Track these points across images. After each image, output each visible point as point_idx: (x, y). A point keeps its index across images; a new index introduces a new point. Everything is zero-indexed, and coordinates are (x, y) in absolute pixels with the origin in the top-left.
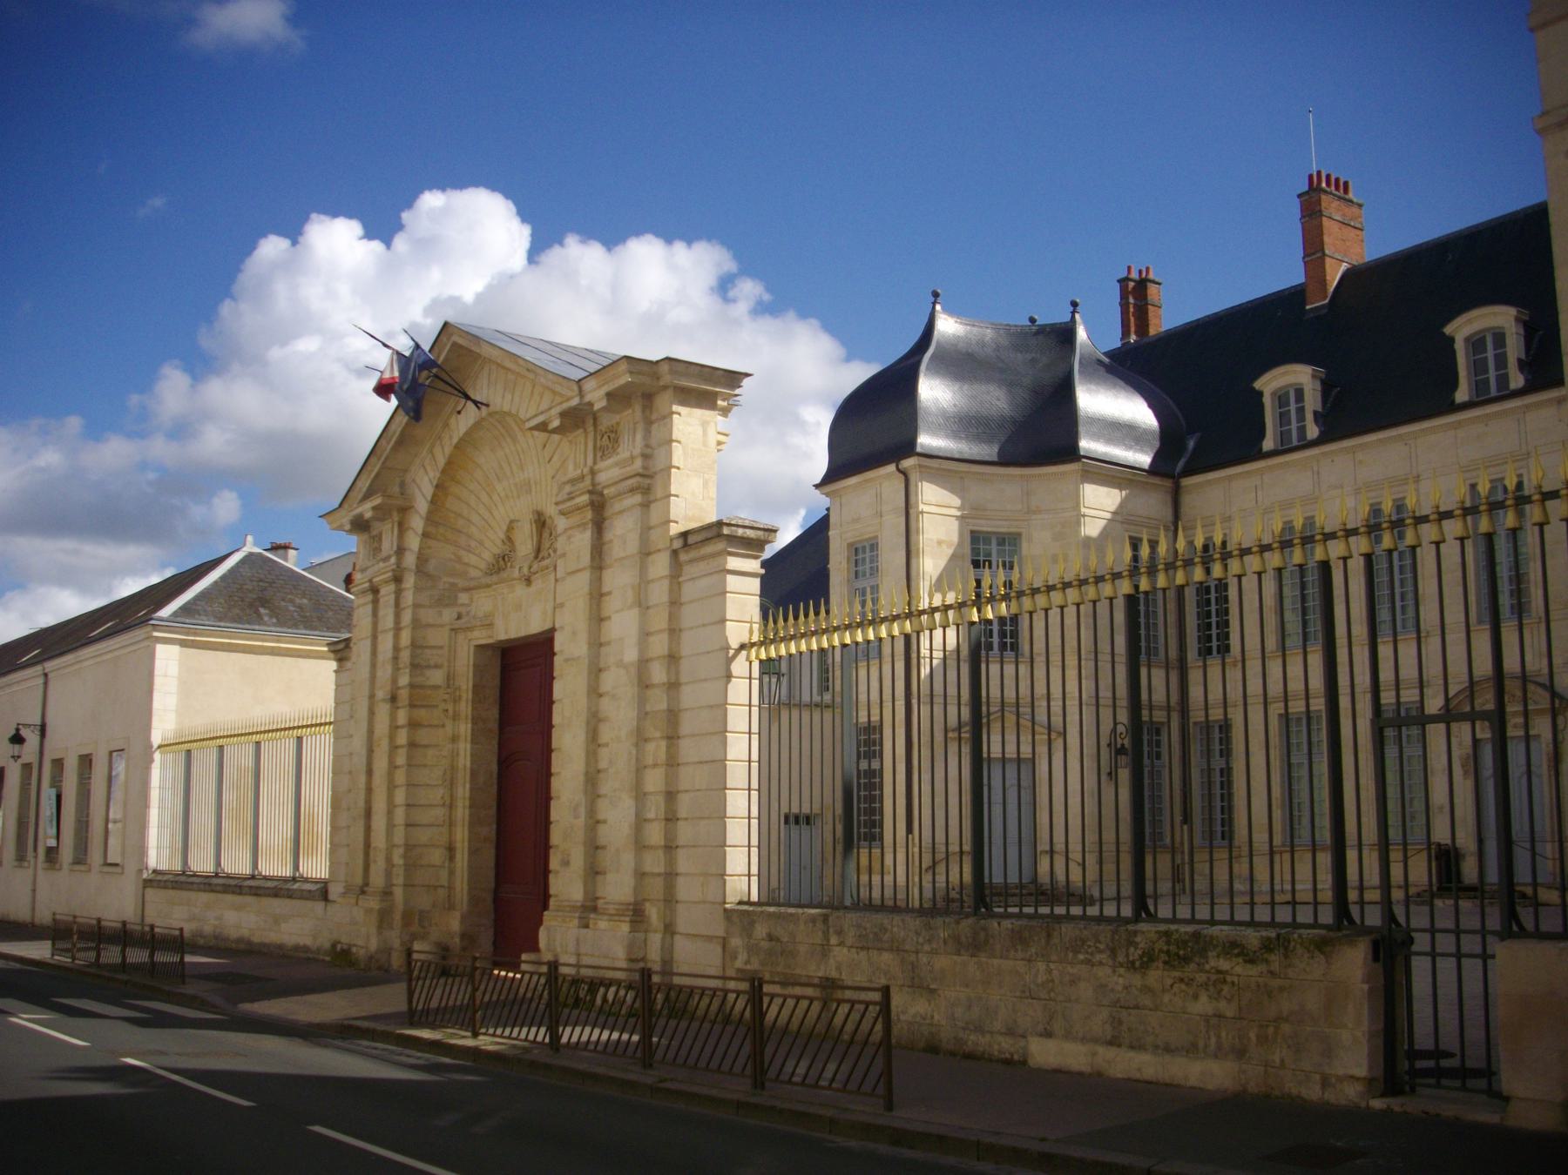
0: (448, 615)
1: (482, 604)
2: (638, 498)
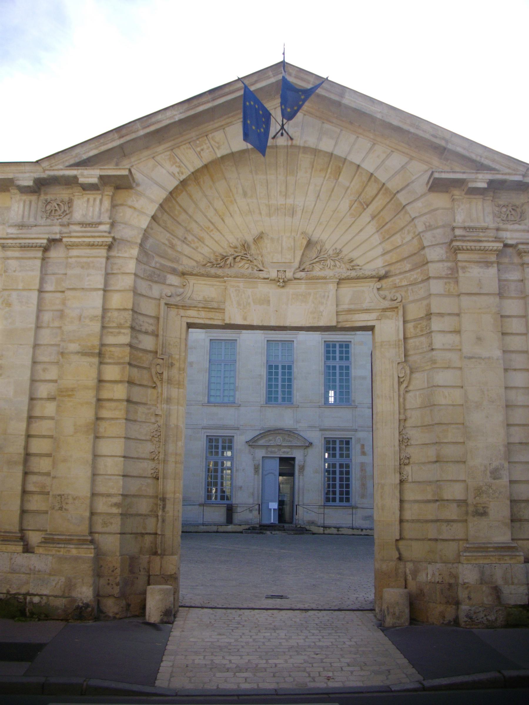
0: (156, 290)
1: (202, 290)
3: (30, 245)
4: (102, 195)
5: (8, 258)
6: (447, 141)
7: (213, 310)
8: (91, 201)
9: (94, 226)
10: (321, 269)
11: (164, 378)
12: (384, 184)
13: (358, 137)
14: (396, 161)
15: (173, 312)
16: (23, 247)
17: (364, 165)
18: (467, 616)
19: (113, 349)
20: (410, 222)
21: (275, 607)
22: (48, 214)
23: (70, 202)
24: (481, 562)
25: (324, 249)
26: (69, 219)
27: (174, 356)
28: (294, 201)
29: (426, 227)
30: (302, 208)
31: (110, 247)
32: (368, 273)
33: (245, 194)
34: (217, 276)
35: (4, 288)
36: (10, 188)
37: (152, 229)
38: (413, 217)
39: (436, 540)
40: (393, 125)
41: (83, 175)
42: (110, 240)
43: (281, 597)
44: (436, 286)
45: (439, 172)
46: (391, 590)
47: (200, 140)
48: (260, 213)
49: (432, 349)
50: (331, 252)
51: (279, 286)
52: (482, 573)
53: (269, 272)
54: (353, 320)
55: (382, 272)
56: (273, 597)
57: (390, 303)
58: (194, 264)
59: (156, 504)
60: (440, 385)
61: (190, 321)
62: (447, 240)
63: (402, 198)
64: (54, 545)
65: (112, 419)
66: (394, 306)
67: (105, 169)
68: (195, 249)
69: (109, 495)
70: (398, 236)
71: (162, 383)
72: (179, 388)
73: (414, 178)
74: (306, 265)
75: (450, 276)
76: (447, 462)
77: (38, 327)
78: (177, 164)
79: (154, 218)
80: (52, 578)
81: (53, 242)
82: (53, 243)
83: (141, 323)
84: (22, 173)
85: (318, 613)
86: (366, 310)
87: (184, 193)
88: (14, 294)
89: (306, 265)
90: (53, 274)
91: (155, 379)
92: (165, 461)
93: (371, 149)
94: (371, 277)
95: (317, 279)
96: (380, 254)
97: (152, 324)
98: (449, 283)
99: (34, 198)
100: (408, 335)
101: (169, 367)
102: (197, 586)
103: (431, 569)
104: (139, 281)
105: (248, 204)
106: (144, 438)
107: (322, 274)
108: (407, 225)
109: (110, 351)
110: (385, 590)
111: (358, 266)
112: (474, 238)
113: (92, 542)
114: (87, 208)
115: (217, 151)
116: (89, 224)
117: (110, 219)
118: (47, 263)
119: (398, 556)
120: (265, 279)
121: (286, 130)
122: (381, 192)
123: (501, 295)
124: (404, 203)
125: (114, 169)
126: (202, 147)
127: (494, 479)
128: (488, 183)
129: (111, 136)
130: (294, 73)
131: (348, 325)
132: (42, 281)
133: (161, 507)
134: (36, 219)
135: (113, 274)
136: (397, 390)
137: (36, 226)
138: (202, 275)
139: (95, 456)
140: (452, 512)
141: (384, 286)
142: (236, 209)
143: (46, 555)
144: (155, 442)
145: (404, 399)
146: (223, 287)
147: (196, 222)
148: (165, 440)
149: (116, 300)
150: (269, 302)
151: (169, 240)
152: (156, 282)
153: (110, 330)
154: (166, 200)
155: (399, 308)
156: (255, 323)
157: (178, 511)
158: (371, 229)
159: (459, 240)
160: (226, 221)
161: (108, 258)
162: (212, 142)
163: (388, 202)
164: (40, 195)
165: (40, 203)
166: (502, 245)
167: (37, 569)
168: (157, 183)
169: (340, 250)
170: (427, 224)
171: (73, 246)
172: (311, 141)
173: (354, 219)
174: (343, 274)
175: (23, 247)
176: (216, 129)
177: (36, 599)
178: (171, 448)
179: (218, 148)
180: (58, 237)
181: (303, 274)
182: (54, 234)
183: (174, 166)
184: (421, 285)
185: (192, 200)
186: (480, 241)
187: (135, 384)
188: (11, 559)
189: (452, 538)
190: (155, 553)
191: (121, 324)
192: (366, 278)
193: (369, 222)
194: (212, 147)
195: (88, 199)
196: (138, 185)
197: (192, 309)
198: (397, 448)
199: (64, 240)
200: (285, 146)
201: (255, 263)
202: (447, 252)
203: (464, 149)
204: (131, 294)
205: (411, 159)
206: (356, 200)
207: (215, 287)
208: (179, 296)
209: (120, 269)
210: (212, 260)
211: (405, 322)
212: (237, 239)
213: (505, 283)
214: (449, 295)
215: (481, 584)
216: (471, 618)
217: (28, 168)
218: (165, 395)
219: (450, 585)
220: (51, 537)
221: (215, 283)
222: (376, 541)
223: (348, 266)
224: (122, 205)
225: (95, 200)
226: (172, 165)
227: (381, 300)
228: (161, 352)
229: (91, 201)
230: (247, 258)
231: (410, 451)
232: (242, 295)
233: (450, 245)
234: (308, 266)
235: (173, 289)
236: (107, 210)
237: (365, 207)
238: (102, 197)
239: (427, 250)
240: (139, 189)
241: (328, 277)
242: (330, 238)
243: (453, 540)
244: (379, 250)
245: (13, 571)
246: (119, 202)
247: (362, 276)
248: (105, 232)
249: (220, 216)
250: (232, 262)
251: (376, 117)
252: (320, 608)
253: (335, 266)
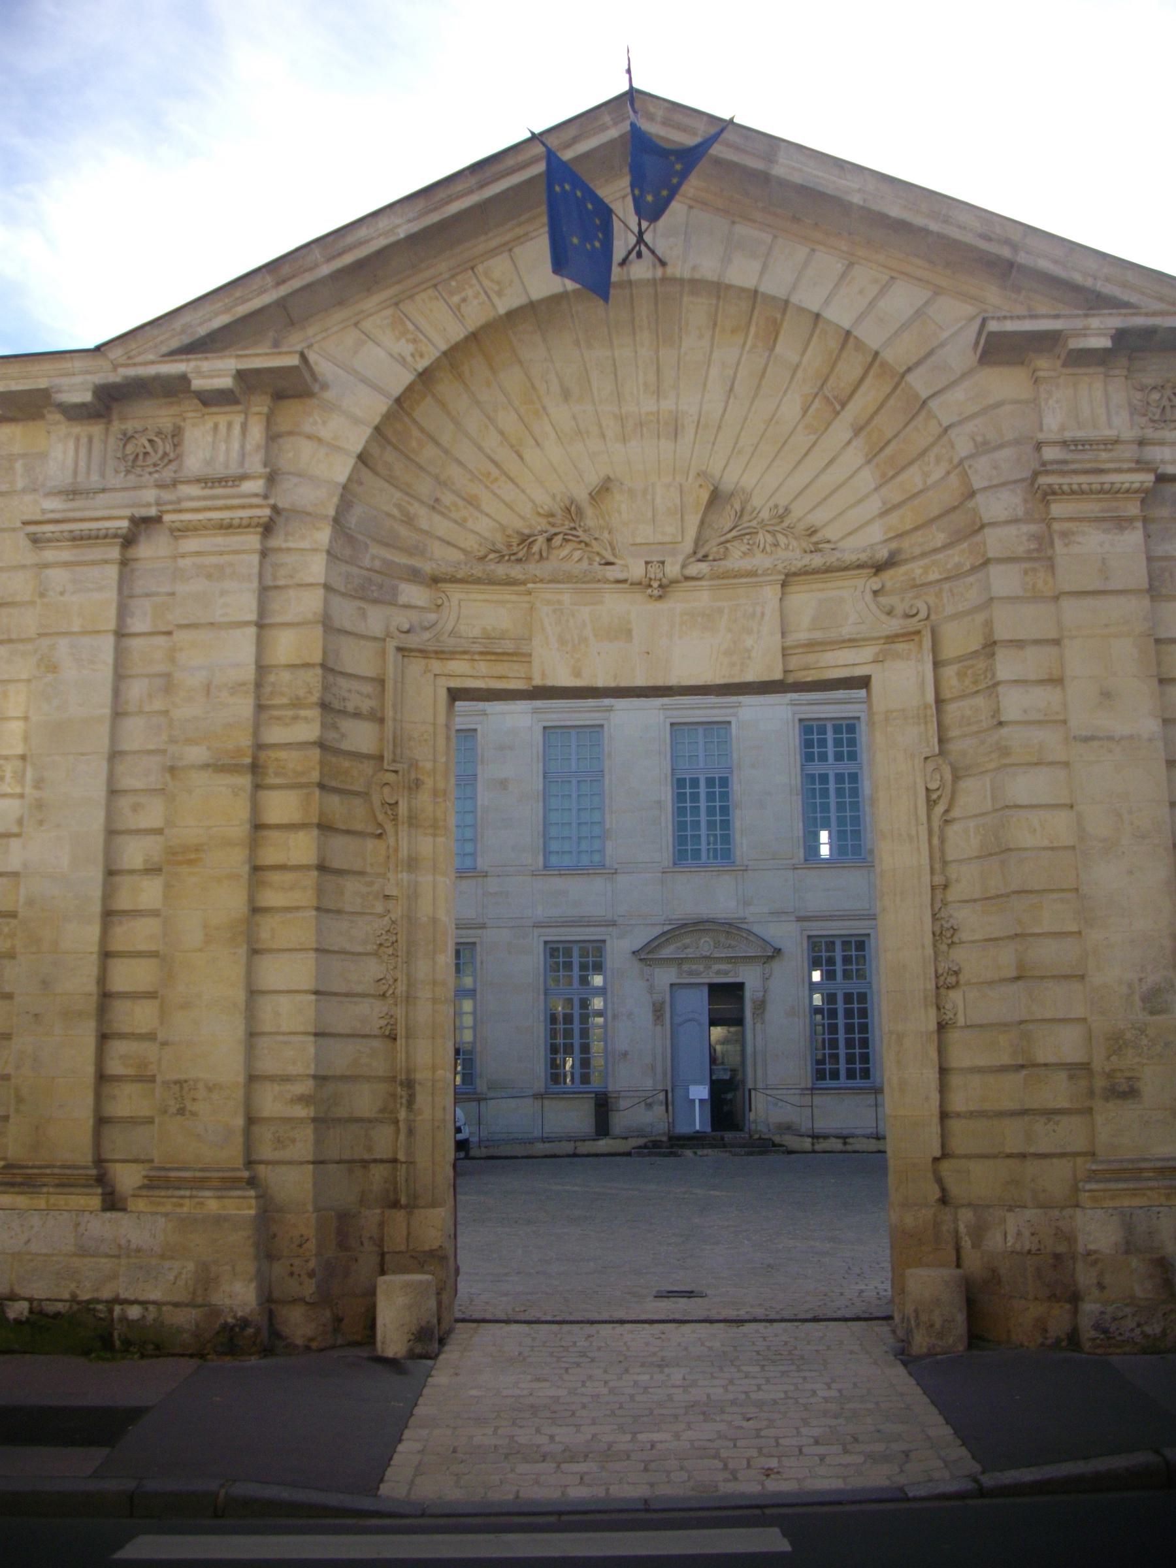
0: (376, 620)
1: (480, 613)
3: (94, 533)
4: (246, 415)
5: (46, 566)
6: (1015, 247)
7: (505, 658)
8: (223, 428)
9: (230, 483)
10: (744, 554)
11: (400, 813)
12: (876, 354)
13: (813, 250)
14: (902, 300)
15: (415, 667)
16: (78, 539)
17: (830, 314)
18: (1097, 1327)
19: (283, 754)
20: (940, 437)
21: (671, 1317)
22: (130, 463)
23: (177, 434)
24: (1126, 1203)
25: (749, 508)
26: (175, 472)
27: (421, 764)
28: (677, 404)
29: (976, 446)
30: (696, 418)
31: (268, 529)
32: (850, 558)
33: (566, 395)
34: (510, 582)
35: (41, 631)
36: (45, 412)
37: (360, 483)
38: (945, 424)
39: (1023, 1156)
40: (888, 217)
41: (200, 374)
42: (267, 512)
43: (690, 1294)
44: (1004, 580)
45: (999, 318)
46: (923, 1272)
47: (459, 278)
48: (603, 436)
49: (1001, 724)
50: (765, 514)
51: (651, 596)
52: (1128, 1228)
53: (626, 566)
54: (823, 664)
55: (883, 554)
56: (671, 1294)
57: (902, 622)
58: (462, 557)
59: (393, 1095)
60: (1020, 802)
61: (455, 683)
62: (1027, 474)
63: (919, 383)
64: (170, 1192)
65: (287, 909)
66: (911, 629)
67: (246, 356)
68: (461, 523)
69: (286, 1079)
70: (914, 470)
71: (396, 825)
72: (435, 835)
73: (945, 335)
74: (711, 547)
75: (1035, 555)
76: (1043, 978)
77: (118, 714)
78: (410, 336)
79: (363, 458)
80: (167, 1264)
81: (143, 524)
82: (143, 526)
83: (346, 694)
84: (67, 375)
85: (766, 1327)
86: (850, 640)
87: (429, 400)
88: (63, 644)
89: (711, 547)
90: (147, 595)
91: (381, 817)
92: (410, 999)
93: (843, 276)
94: (859, 567)
95: (735, 577)
96: (876, 513)
97: (369, 696)
98: (1034, 570)
99: (97, 429)
100: (947, 694)
101: (410, 788)
102: (506, 1274)
103: (1013, 1222)
104: (336, 600)
105: (574, 418)
106: (359, 949)
107: (746, 564)
108: (933, 444)
109: (276, 759)
110: (910, 1272)
111: (828, 542)
112: (1088, 466)
113: (252, 1182)
114: (214, 444)
115: (496, 299)
116: (220, 480)
117: (265, 466)
118: (132, 571)
119: (937, 1194)
120: (618, 582)
121: (650, 245)
122: (871, 373)
123: (1154, 591)
124: (924, 395)
125: (267, 354)
126: (463, 294)
127: (1152, 1013)
128: (1113, 338)
129: (258, 281)
130: (660, 114)
131: (810, 676)
132: (123, 611)
133: (404, 1101)
134: (103, 475)
135: (277, 587)
136: (924, 819)
137: (104, 490)
138: (478, 581)
139: (253, 993)
140: (1057, 1092)
141: (889, 584)
142: (548, 428)
143: (152, 1214)
144: (385, 957)
145: (942, 840)
146: (527, 605)
148: (408, 952)
149: (287, 646)
150: (629, 633)
151: (398, 506)
152: (376, 601)
153: (275, 713)
154: (388, 417)
155: (924, 632)
156: (600, 683)
157: (444, 1109)
158: (854, 457)
159: (1053, 472)
160: (527, 457)
161: (264, 554)
162: (486, 283)
163: (888, 396)
164: (109, 422)
165: (112, 440)
166: (1151, 477)
167: (133, 1246)
168: (364, 380)
169: (787, 510)
170: (979, 439)
171: (187, 530)
172: (708, 267)
173: (813, 437)
174: (794, 562)
175: (78, 539)
176: (493, 253)
177: (134, 1312)
178: (422, 969)
179: (500, 294)
180: (153, 512)
181: (704, 567)
182: (144, 506)
183: (403, 341)
184: (971, 579)
185: (448, 413)
187: (337, 830)
188: (78, 1225)
189: (1058, 1150)
190: (395, 1205)
191: (298, 698)
192: (846, 569)
193: (849, 442)
194: (486, 293)
195: (216, 427)
196: (325, 387)
197: (458, 656)
198: (930, 951)
199: (167, 518)
200: (648, 280)
201: (596, 547)
202: (1025, 501)
203: (1056, 262)
204: (319, 631)
205: (936, 294)
206: (816, 395)
207: (509, 606)
208: (426, 629)
209: (291, 577)
210: (499, 546)
211: (936, 664)
212: (554, 496)
213: (1164, 564)
214: (1036, 598)
215: (1127, 1252)
216: (1105, 1331)
217: (79, 364)
218: (404, 853)
219: (1057, 1257)
220: (162, 1173)
221: (508, 597)
222: (892, 1163)
223: (804, 545)
224: (290, 433)
225: (230, 425)
226: (398, 339)
227: (883, 617)
228: (391, 757)
229: (223, 428)
230: (578, 537)
231: (959, 955)
232: (568, 621)
233: (1032, 484)
234: (715, 549)
235: (414, 616)
236: (258, 447)
237: (838, 408)
238: (246, 418)
239: (980, 498)
240: (328, 395)
241: (760, 572)
242: (761, 482)
243: (1063, 1155)
244: (874, 505)
245: (82, 1252)
246: (284, 428)
247: (835, 564)
248: (256, 495)
249: (512, 446)
250: (544, 547)
251: (851, 204)
252: (773, 1316)
253: (776, 545)
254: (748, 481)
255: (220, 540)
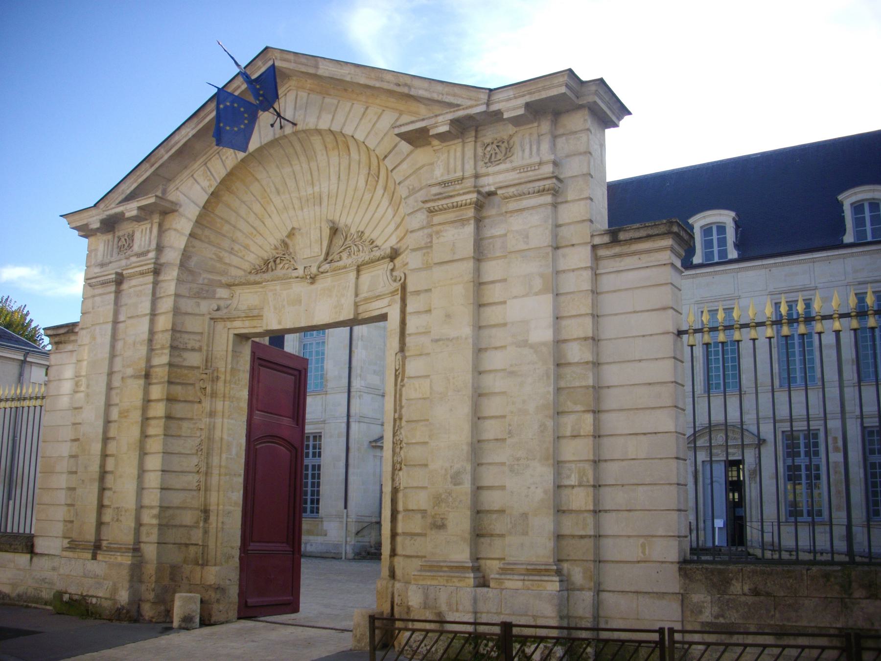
0: (206, 306)
1: (246, 298)
2: (548, 199)
33: (278, 193)
48: (294, 208)
52: (426, 597)
76: (415, 465)
79: (192, 235)
87: (220, 205)
101: (213, 381)
106: (189, 452)
127: (455, 485)
132: (116, 313)
138: (244, 284)
142: (273, 208)
147: (240, 230)
150: (300, 301)
151: (215, 254)
152: (205, 298)
170: (411, 187)
177: (94, 601)
186: (451, 197)
187: (179, 401)
189: (415, 554)
203: (426, 90)
210: (257, 267)
215: (425, 608)
242: (352, 220)
243: (417, 557)
245: (85, 576)
254: (349, 222)
255: (141, 279)
